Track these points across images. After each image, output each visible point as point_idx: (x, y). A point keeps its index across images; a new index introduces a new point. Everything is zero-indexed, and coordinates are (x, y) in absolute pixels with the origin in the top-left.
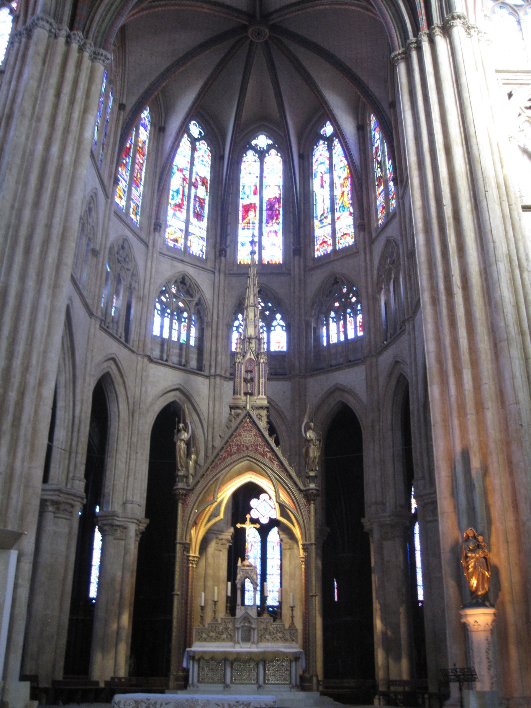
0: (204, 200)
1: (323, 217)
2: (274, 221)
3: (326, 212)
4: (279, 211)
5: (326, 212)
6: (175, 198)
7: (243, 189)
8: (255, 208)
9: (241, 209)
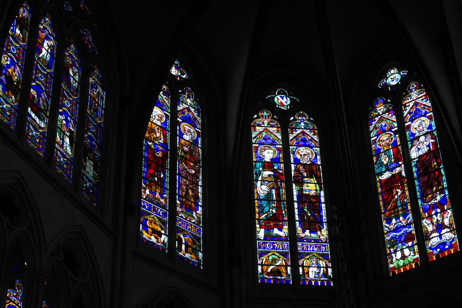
0: (318, 197)
2: (434, 189)
6: (267, 209)
7: (377, 159)
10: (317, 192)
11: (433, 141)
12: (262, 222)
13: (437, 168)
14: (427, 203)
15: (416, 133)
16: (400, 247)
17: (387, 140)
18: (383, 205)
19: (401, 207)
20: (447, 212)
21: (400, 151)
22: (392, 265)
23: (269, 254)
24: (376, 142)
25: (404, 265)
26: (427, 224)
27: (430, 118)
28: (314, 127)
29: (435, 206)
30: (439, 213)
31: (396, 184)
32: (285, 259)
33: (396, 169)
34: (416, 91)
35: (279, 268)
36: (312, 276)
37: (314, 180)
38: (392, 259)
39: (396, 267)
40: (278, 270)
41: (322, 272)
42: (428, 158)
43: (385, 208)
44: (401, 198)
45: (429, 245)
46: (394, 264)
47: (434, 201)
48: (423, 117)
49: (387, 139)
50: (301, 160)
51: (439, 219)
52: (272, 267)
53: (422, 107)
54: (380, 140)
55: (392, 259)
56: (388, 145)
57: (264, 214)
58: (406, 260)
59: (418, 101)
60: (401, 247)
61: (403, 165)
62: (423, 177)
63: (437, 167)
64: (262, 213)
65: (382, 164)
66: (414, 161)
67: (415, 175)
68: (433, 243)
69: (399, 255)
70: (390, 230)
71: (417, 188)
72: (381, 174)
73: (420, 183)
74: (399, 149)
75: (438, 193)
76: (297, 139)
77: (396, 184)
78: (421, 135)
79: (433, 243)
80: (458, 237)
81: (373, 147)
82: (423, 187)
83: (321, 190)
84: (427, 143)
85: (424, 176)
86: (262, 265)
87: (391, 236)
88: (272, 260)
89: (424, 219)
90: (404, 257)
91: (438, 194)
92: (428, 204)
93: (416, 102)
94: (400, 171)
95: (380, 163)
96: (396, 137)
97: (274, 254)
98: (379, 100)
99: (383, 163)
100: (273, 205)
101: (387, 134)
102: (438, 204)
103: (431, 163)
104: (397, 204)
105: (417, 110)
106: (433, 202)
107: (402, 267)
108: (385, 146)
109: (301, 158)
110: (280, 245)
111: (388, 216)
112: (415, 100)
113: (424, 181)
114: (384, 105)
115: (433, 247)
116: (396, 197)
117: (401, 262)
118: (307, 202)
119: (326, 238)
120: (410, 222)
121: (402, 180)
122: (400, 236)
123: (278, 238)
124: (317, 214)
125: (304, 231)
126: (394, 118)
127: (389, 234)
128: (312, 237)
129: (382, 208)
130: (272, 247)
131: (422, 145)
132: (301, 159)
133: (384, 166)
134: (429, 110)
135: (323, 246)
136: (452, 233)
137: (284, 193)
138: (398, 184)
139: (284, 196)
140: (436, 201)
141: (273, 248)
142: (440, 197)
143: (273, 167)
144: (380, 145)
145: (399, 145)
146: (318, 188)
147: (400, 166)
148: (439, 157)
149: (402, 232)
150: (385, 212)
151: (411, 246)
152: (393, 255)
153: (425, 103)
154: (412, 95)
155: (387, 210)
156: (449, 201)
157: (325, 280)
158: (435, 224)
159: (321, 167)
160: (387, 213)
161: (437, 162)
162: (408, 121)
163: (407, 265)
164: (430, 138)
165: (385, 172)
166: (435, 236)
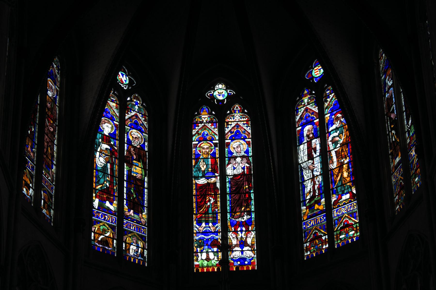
1: (313, 202)
2: (243, 209)
3: (317, 194)
5: (317, 194)
6: (102, 181)
7: (196, 163)
10: (142, 176)
11: (248, 165)
12: (98, 193)
13: (248, 191)
14: (235, 219)
15: (234, 153)
16: (206, 250)
17: (207, 148)
18: (195, 207)
19: (211, 214)
21: (217, 164)
22: (197, 262)
23: (101, 224)
24: (196, 147)
25: (208, 266)
27: (248, 143)
28: (145, 113)
29: (241, 224)
30: (244, 231)
31: (209, 192)
32: (113, 232)
33: (211, 179)
34: (239, 114)
35: (107, 239)
36: (132, 253)
37: (140, 164)
38: (197, 257)
39: (200, 265)
40: (107, 241)
41: (139, 251)
42: (241, 179)
43: (197, 211)
44: (213, 206)
45: (232, 256)
47: (241, 219)
48: (242, 140)
49: (207, 148)
50: (132, 142)
51: (243, 236)
52: (102, 237)
53: (242, 130)
54: (201, 146)
55: (198, 258)
56: (207, 154)
57: (100, 185)
59: (240, 123)
60: (206, 249)
61: (218, 177)
62: (234, 195)
63: (248, 191)
64: (98, 183)
65: (199, 169)
66: (229, 177)
67: (228, 190)
68: (235, 255)
69: (204, 256)
70: (200, 231)
71: (228, 203)
72: (197, 178)
73: (231, 199)
74: (217, 161)
76: (131, 120)
77: (209, 192)
78: (238, 156)
79: (235, 255)
80: (257, 258)
81: (194, 151)
82: (233, 204)
83: (145, 176)
84: (242, 166)
86: (95, 233)
87: (199, 237)
89: (230, 232)
90: (208, 259)
91: (245, 214)
92: (236, 220)
93: (237, 124)
94: (215, 181)
95: (197, 168)
96: (216, 149)
97: (104, 225)
98: (204, 108)
99: (201, 169)
100: (107, 178)
101: (207, 143)
102: (244, 223)
103: (243, 184)
104: (208, 210)
105: (238, 131)
106: (240, 220)
107: (205, 267)
108: (204, 153)
109: (133, 140)
110: (110, 218)
111: (199, 218)
112: (237, 122)
113: (235, 199)
114: (208, 115)
115: (235, 259)
116: (209, 204)
117: (205, 263)
118: (133, 184)
119: (146, 221)
120: (218, 230)
121: (216, 191)
122: (208, 240)
123: (109, 211)
125: (129, 211)
126: (216, 131)
127: (198, 234)
128: (135, 217)
129: (195, 209)
130: (103, 218)
131: (238, 166)
132: (133, 141)
133: (201, 172)
134: (248, 136)
135: (143, 228)
136: (252, 252)
137: (117, 170)
138: (211, 193)
139: (116, 172)
140: (243, 220)
141: (104, 219)
143: (110, 142)
144: (200, 151)
145: (218, 158)
146: (143, 174)
147: (216, 177)
148: (251, 181)
149: (210, 237)
150: (196, 214)
151: (216, 252)
152: (199, 254)
153: (245, 128)
154: (235, 116)
155: (199, 213)
156: (254, 224)
158: (239, 240)
159: (147, 153)
160: (198, 215)
161: (249, 186)
162: (228, 138)
163: (210, 267)
165: (201, 177)
166: (238, 250)
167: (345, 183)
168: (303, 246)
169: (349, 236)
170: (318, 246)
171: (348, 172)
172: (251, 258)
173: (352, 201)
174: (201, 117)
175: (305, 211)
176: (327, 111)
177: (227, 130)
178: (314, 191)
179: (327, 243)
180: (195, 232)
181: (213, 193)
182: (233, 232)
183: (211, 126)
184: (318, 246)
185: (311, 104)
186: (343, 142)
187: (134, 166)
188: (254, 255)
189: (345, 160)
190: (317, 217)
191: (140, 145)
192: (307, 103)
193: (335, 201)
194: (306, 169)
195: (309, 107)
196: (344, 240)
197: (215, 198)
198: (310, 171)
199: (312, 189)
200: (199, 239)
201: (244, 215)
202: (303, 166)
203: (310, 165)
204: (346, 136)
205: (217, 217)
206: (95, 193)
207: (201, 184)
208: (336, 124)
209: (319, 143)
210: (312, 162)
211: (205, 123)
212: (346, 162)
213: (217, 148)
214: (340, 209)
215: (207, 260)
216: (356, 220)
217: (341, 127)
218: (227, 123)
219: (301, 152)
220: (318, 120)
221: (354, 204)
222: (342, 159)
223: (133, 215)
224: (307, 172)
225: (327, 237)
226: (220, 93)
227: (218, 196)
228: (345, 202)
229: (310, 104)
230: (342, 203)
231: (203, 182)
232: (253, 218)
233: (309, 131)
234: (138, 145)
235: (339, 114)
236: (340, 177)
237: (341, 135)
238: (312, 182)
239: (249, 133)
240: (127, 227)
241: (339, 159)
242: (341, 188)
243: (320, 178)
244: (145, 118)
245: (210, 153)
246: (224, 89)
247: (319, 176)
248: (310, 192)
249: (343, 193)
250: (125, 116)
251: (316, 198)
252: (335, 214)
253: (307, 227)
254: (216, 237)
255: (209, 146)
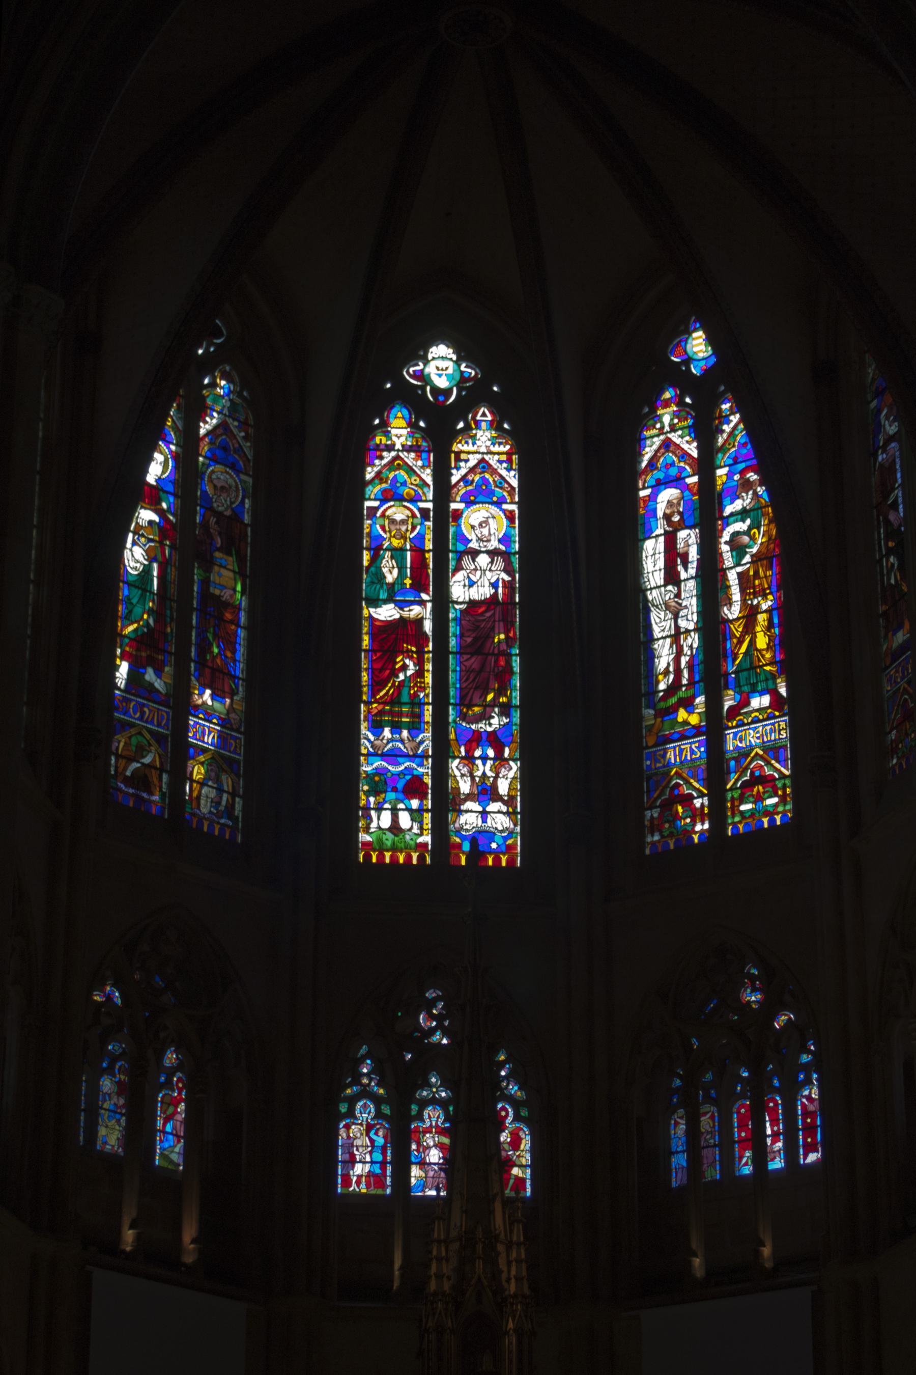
1: (673, 700)
2: (490, 697)
3: (685, 682)
4: (510, 655)
5: (685, 682)
6: (138, 610)
8: (419, 638)
9: (366, 642)
11: (507, 578)
13: (504, 650)
14: (469, 724)
15: (471, 540)
18: (367, 683)
19: (408, 706)
20: (509, 764)
21: (426, 566)
22: (366, 835)
24: (375, 515)
25: (394, 849)
26: (461, 774)
27: (510, 516)
28: (247, 418)
30: (491, 759)
31: (405, 645)
32: (160, 750)
33: (411, 608)
37: (231, 562)
39: (376, 846)
41: (224, 803)
42: (488, 614)
43: (374, 691)
44: (412, 685)
46: (371, 835)
47: (483, 726)
48: (493, 507)
49: (403, 522)
50: (214, 500)
51: (489, 773)
52: (135, 765)
53: (496, 479)
55: (370, 824)
57: (132, 623)
58: (401, 839)
59: (490, 459)
61: (429, 605)
63: (505, 648)
64: (129, 620)
66: (457, 607)
68: (466, 824)
70: (376, 751)
72: (375, 602)
74: (428, 561)
75: (496, 710)
77: (405, 645)
79: (466, 824)
81: (367, 526)
84: (492, 577)
85: (472, 655)
86: (118, 757)
87: (375, 766)
88: (137, 747)
89: (455, 758)
90: (395, 828)
92: (470, 727)
93: (483, 460)
96: (425, 526)
97: (140, 734)
99: (385, 577)
106: (481, 728)
107: (388, 851)
108: (394, 535)
109: (215, 494)
110: (154, 715)
111: (376, 715)
112: (483, 453)
113: (471, 670)
115: (464, 833)
116: (401, 677)
117: (389, 838)
119: (241, 719)
124: (229, 654)
127: (371, 759)
130: (138, 715)
132: (215, 497)
133: (385, 587)
136: (510, 818)
141: (141, 718)
142: (498, 723)
145: (429, 551)
147: (422, 603)
148: (513, 626)
151: (416, 811)
153: (504, 473)
157: (228, 826)
158: (477, 781)
159: (249, 529)
160: (374, 705)
162: (458, 499)
164: (502, 568)
165: (386, 601)
166: (474, 810)
167: (761, 664)
168: (644, 816)
169: (763, 810)
170: (681, 822)
171: (768, 635)
172: (506, 834)
173: (775, 717)
174: (390, 432)
175: (653, 722)
176: (720, 458)
177: (455, 477)
178: (678, 672)
179: (706, 818)
180: (364, 751)
181: (414, 649)
182: (462, 758)
183: (416, 459)
184: (683, 824)
185: (680, 432)
186: (759, 551)
187: (216, 568)
188: (515, 825)
189: (762, 602)
190: (682, 745)
191: (233, 510)
192: (670, 425)
193: (731, 707)
194: (660, 607)
195: (674, 439)
196: (750, 817)
197: (420, 663)
198: (670, 615)
199: (671, 663)
200: (375, 771)
201: (493, 714)
202: (650, 598)
203: (670, 599)
204: (769, 536)
205: (420, 716)
206: (121, 647)
207: (384, 619)
208: (744, 500)
209: (695, 542)
210: (675, 590)
211: (398, 450)
212: (764, 606)
213: (430, 524)
214: (743, 733)
215: (393, 830)
216: (783, 770)
217: (757, 509)
218: (458, 454)
219: (646, 557)
220: (695, 479)
221: (779, 725)
222: (755, 597)
223: (210, 702)
224: (662, 616)
225: (706, 801)
226: (442, 370)
227: (426, 656)
228: (757, 714)
229: (677, 430)
230: (750, 716)
231: (390, 616)
232: (516, 724)
233: (671, 506)
234: (226, 509)
235: (752, 474)
236: (748, 647)
237: (754, 533)
238: (674, 646)
239: (513, 488)
240: (194, 737)
241: (748, 598)
242: (748, 677)
243: (694, 640)
244: (247, 433)
245: (409, 537)
246: (451, 359)
247: (692, 634)
248: (666, 672)
249: (754, 690)
250: (199, 427)
251: (681, 692)
252: (731, 744)
253: (655, 765)
254: (418, 769)
255: (408, 516)
